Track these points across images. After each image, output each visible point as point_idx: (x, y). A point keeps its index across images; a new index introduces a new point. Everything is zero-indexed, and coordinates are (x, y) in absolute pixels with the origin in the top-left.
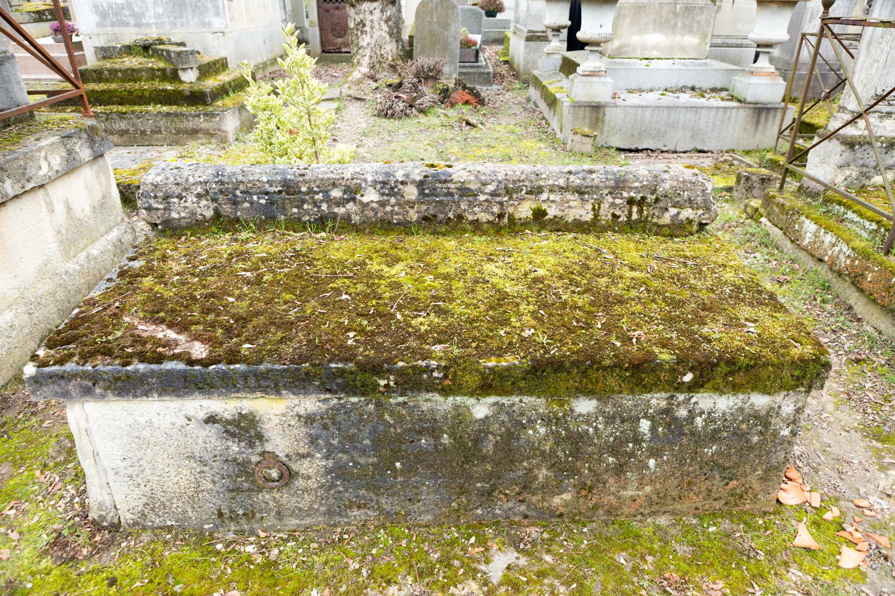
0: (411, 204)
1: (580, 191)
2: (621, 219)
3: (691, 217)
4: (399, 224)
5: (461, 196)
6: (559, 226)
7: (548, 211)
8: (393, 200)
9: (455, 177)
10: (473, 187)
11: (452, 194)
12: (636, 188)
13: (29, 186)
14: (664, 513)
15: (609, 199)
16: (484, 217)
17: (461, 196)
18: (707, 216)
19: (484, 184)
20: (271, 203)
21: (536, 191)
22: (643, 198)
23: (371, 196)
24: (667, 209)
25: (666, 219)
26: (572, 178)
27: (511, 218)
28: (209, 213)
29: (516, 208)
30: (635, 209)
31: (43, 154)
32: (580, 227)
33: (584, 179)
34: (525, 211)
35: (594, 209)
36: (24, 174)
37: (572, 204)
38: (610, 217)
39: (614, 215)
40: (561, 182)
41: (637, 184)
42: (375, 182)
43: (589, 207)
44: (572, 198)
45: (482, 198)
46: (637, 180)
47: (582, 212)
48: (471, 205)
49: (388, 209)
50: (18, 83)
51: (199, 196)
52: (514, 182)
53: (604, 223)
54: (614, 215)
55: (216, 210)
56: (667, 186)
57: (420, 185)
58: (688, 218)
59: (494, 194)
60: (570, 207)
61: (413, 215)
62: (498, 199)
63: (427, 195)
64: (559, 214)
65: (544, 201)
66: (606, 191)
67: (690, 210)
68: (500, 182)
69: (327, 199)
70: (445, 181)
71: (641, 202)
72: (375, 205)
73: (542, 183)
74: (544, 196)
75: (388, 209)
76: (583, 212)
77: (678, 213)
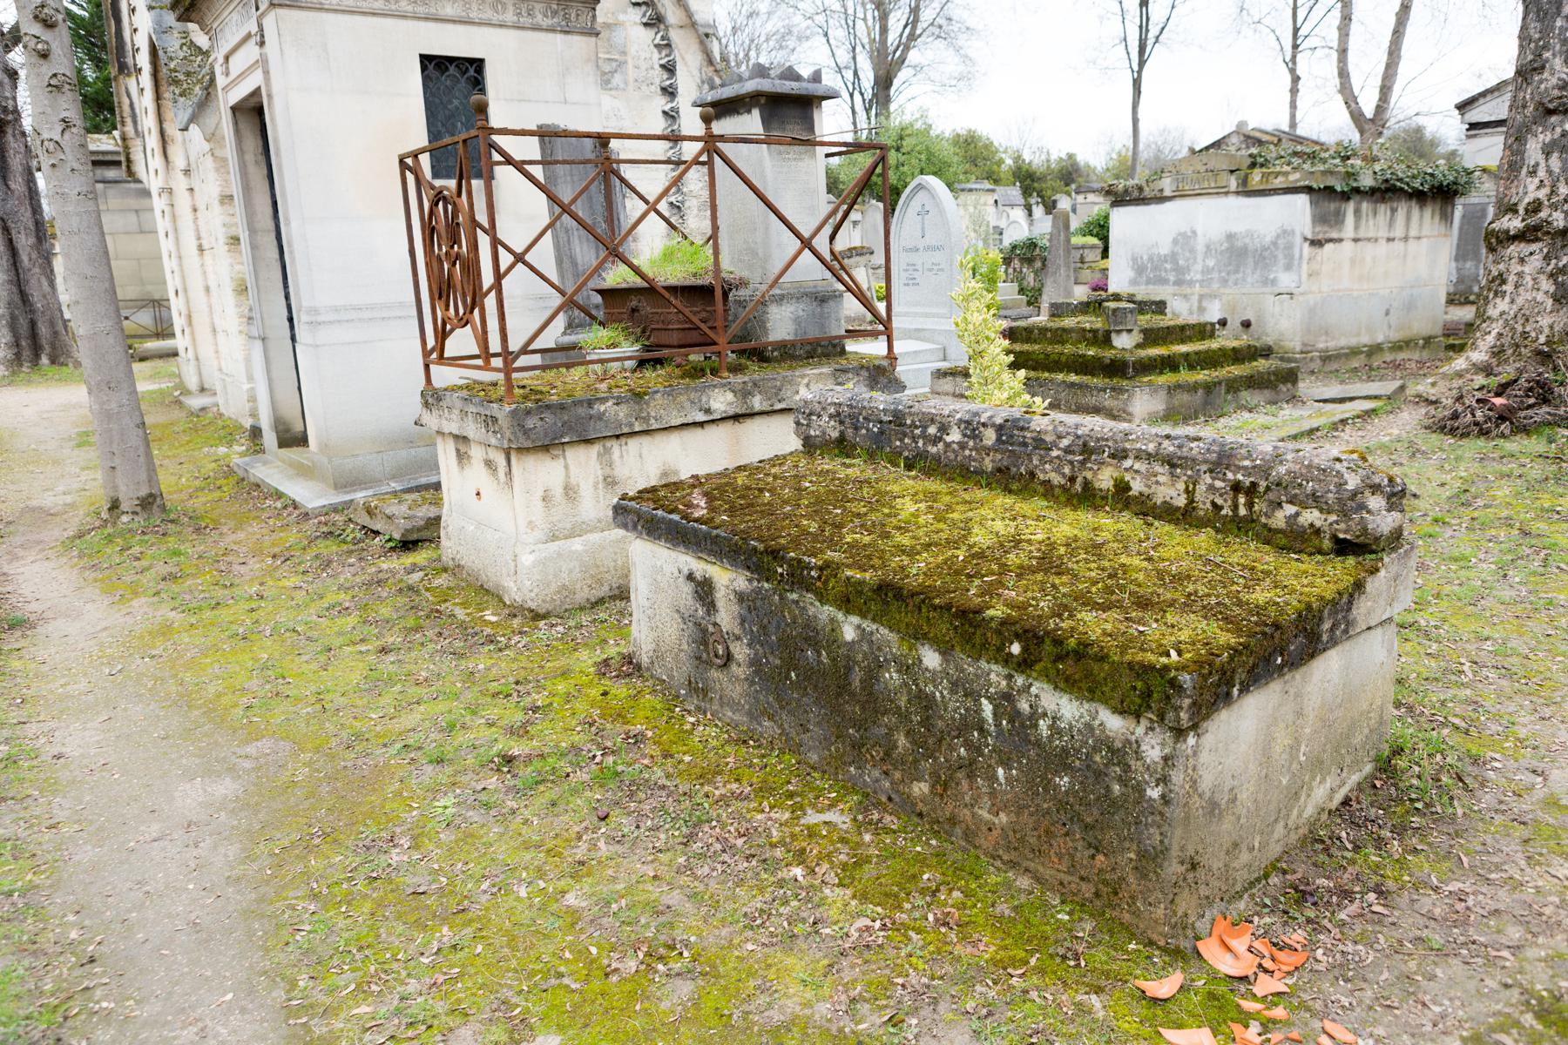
0: (988, 450)
1: (1171, 463)
2: (1224, 512)
3: (1318, 524)
4: (975, 472)
5: (1035, 448)
6: (1146, 509)
7: (1132, 484)
8: (971, 443)
9: (1033, 426)
10: (1049, 438)
11: (1025, 444)
12: (1245, 468)
13: (779, 406)
14: (1027, 870)
15: (1208, 479)
16: (1056, 479)
17: (1035, 448)
18: (1343, 526)
19: (1060, 437)
20: (882, 432)
21: (1119, 455)
22: (1254, 485)
23: (955, 436)
24: (1280, 505)
25: (1279, 519)
26: (1166, 443)
27: (1087, 484)
28: (835, 434)
29: (1095, 474)
30: (1242, 500)
31: (806, 381)
32: (1168, 513)
33: (1180, 447)
34: (1105, 479)
35: (1187, 491)
36: (776, 394)
37: (1161, 479)
38: (1209, 505)
39: (1214, 504)
40: (1151, 447)
41: (1247, 463)
42: (960, 420)
43: (1181, 486)
44: (1160, 470)
45: (1055, 453)
46: (1249, 456)
47: (1170, 491)
48: (1043, 461)
49: (967, 452)
50: (838, 320)
51: (831, 416)
52: (1098, 440)
53: (1202, 513)
54: (1214, 504)
55: (842, 433)
56: (1282, 470)
57: (1000, 429)
58: (1312, 525)
59: (1068, 451)
60: (1157, 483)
61: (988, 465)
62: (1070, 457)
63: (1004, 443)
64: (1146, 491)
65: (1126, 470)
66: (1204, 467)
67: (1316, 513)
68: (1078, 437)
69: (924, 436)
70: (1022, 429)
71: (1252, 490)
72: (955, 446)
73: (1128, 446)
74: (1128, 463)
75: (967, 452)
76: (1174, 494)
77: (1297, 514)
